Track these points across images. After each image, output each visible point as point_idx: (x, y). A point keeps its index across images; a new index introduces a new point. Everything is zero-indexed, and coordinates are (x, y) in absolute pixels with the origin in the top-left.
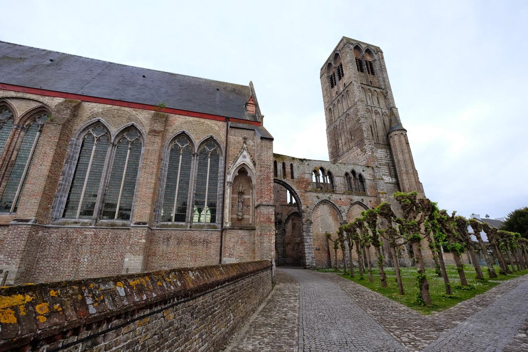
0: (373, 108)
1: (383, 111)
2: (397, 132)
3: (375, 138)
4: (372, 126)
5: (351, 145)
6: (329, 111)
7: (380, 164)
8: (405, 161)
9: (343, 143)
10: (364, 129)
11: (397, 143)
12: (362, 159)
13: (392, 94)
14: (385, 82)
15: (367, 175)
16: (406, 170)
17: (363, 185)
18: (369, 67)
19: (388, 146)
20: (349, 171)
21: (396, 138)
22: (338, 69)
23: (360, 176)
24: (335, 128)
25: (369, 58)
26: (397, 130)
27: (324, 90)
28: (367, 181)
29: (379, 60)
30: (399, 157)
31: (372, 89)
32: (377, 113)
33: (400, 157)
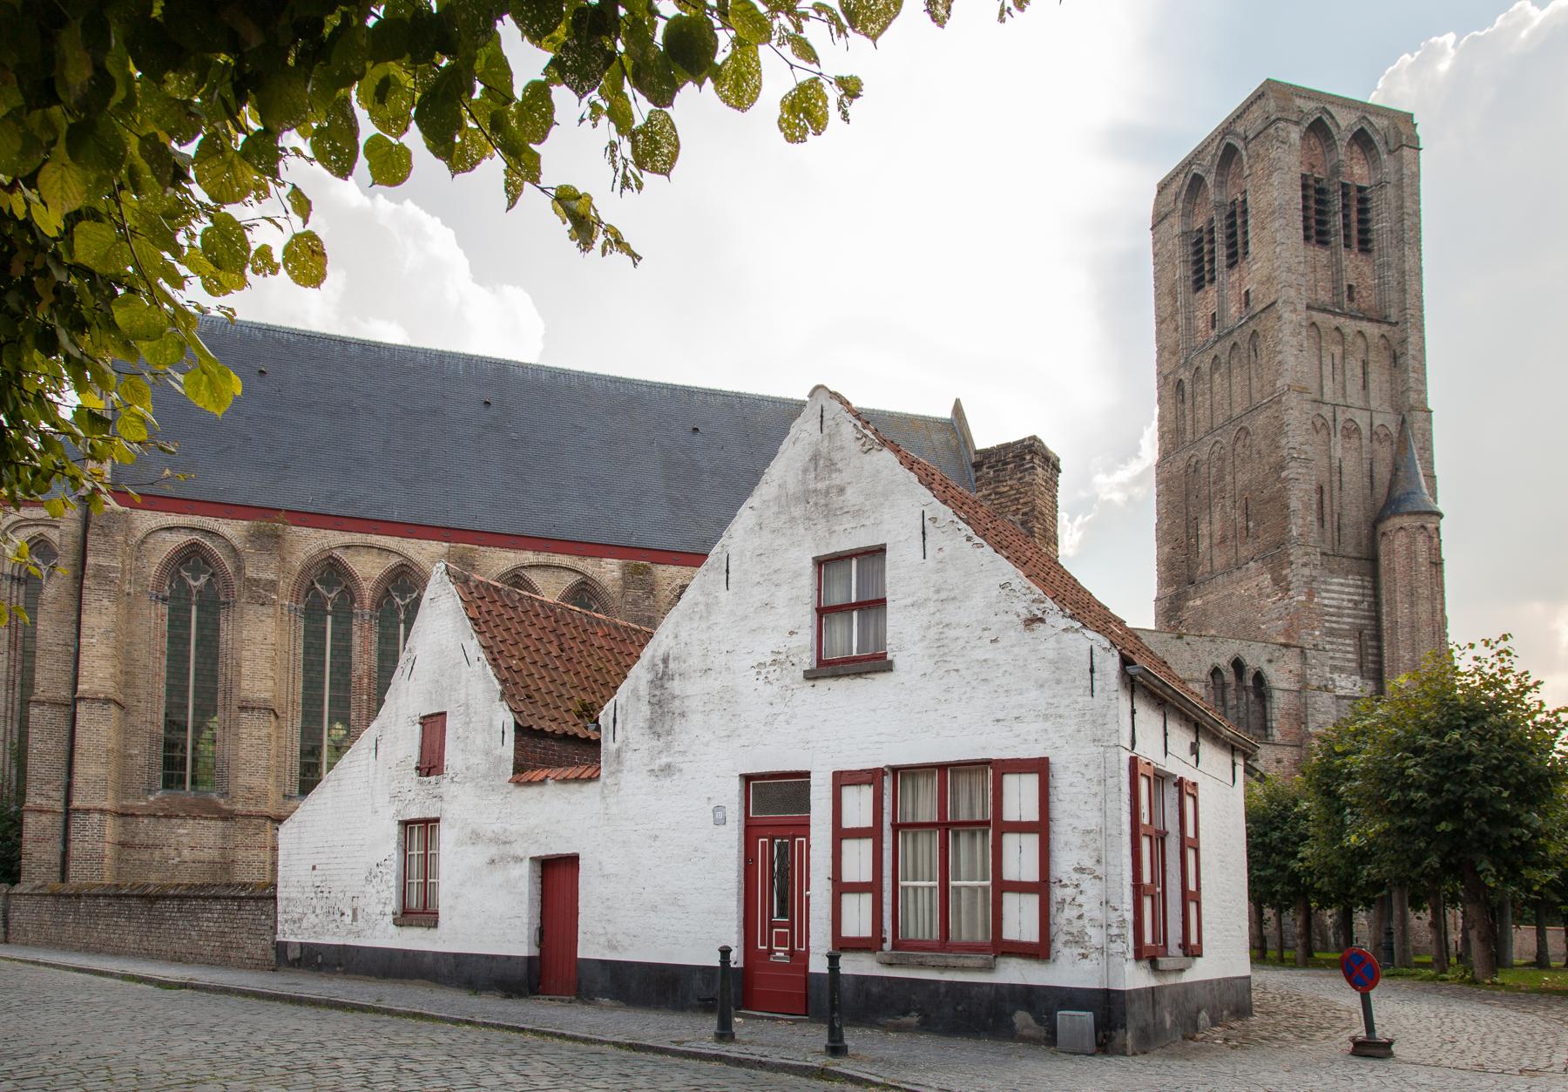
0: (1339, 413)
1: (1377, 422)
2: (1406, 521)
3: (1329, 535)
4: (1326, 488)
5: (1244, 552)
6: (1177, 391)
7: (1331, 632)
8: (1414, 628)
9: (1217, 538)
10: (1294, 504)
11: (1400, 563)
12: (1272, 612)
13: (1422, 350)
14: (1404, 291)
15: (1280, 678)
16: (1411, 659)
17: (1264, 707)
18: (1354, 216)
19: (1370, 564)
20: (1224, 662)
21: (1400, 541)
22: (1232, 215)
23: (1259, 677)
24: (1193, 469)
25: (1359, 173)
26: (1410, 514)
27: (1164, 291)
28: (1277, 694)
29: (1399, 185)
30: (1399, 610)
31: (1350, 326)
32: (1351, 431)
33: (1402, 611)
